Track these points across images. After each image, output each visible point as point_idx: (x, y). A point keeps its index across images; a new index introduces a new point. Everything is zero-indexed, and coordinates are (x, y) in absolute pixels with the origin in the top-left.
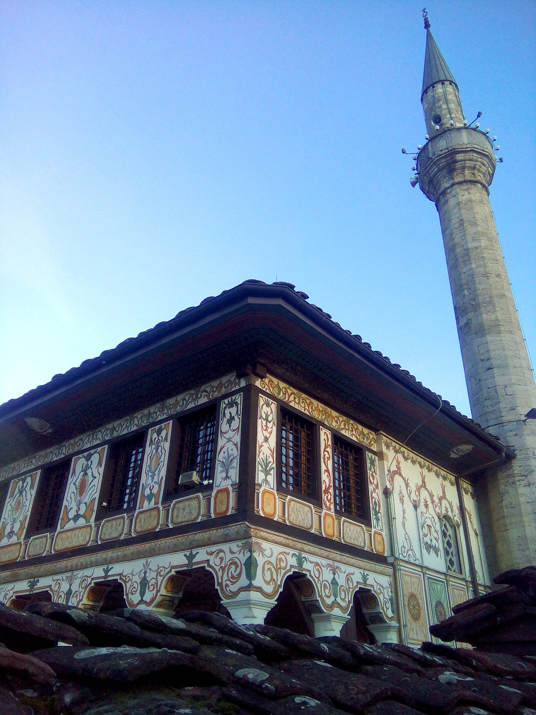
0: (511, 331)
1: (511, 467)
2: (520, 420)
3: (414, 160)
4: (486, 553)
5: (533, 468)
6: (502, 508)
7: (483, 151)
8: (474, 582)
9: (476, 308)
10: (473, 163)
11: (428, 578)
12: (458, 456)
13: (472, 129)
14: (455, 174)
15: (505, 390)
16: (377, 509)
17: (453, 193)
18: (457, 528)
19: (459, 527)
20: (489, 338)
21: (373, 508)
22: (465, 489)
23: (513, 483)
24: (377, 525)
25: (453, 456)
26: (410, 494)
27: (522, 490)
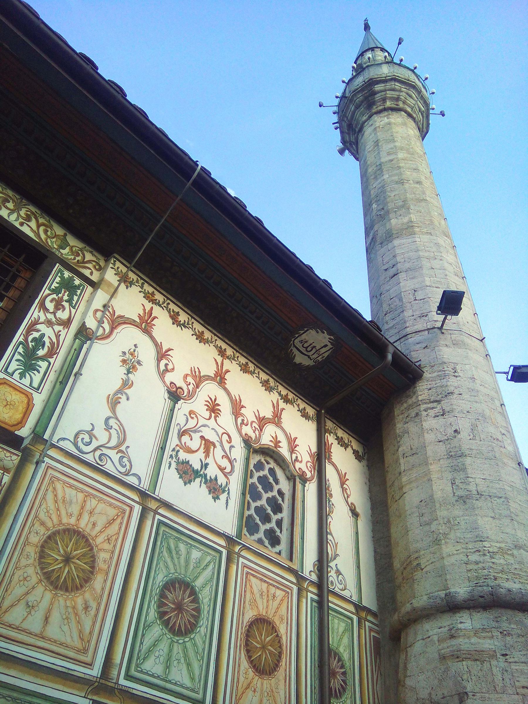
0: (430, 234)
1: (414, 393)
2: (434, 328)
3: (334, 113)
4: (375, 552)
5: (451, 389)
6: (397, 461)
7: (408, 80)
8: (321, 585)
9: (384, 215)
10: (397, 93)
11: (160, 522)
12: (311, 363)
13: (396, 64)
14: (375, 107)
15: (414, 295)
16: (41, 353)
17: (370, 123)
18: (298, 480)
19: (304, 480)
20: (396, 242)
21: (25, 344)
22: (340, 441)
23: (417, 415)
24: (22, 375)
25: (299, 359)
26: (166, 370)
27: (430, 422)
